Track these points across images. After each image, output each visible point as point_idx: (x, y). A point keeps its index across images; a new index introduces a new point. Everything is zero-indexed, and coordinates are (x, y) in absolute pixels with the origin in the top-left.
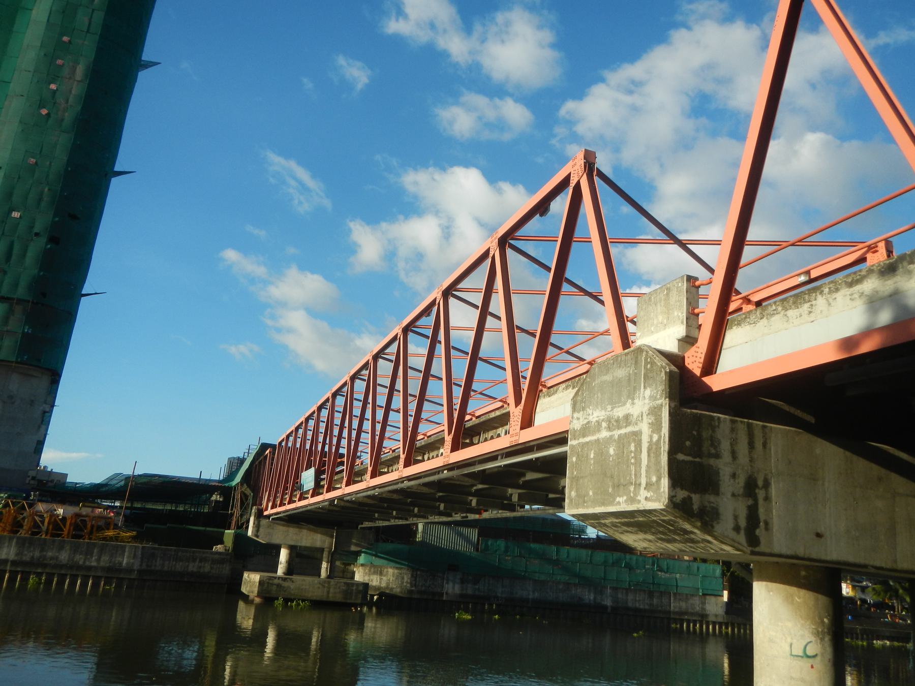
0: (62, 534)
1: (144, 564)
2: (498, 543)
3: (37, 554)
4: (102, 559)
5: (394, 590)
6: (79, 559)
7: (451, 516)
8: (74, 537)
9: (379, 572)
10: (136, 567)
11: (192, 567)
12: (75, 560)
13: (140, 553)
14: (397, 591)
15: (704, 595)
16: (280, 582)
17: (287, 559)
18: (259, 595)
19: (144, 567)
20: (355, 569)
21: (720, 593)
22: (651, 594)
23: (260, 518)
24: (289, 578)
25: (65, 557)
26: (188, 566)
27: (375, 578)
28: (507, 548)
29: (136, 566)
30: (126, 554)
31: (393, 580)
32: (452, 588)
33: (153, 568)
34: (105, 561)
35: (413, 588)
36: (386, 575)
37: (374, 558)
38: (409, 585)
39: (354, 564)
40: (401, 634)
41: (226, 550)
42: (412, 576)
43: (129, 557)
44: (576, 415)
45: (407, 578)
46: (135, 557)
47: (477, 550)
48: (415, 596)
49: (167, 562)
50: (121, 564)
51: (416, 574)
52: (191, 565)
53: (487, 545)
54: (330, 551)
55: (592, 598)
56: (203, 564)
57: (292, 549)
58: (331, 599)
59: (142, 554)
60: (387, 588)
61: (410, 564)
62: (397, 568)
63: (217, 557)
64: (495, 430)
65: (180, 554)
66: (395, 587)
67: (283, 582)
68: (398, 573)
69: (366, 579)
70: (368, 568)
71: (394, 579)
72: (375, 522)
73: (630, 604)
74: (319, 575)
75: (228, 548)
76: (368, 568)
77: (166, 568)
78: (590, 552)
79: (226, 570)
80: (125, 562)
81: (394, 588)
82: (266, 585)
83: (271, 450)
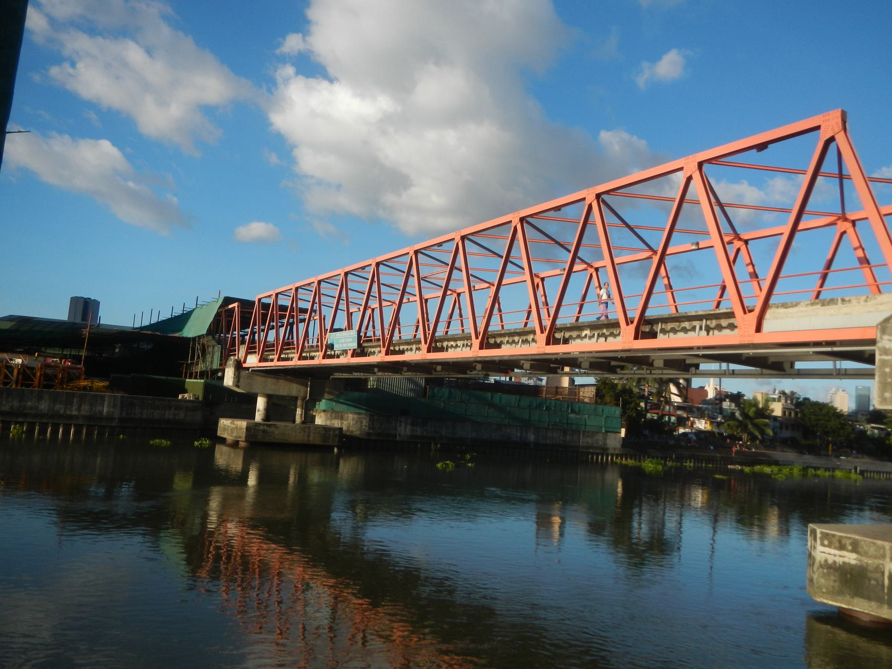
0: (33, 384)
2: (443, 390)
5: (354, 433)
7: (467, 374)
8: (45, 386)
9: (340, 417)
12: (56, 409)
14: (357, 433)
15: (607, 432)
16: (265, 427)
17: (265, 407)
18: (247, 440)
20: (314, 414)
23: (240, 369)
24: (273, 424)
25: (45, 407)
27: (337, 423)
31: (352, 424)
32: (404, 430)
35: (371, 431)
36: (347, 419)
37: (334, 403)
38: (367, 428)
39: (313, 410)
40: (361, 469)
41: (195, 398)
42: (370, 420)
44: (886, 337)
45: (365, 423)
48: (373, 438)
51: (374, 419)
54: (304, 398)
57: (269, 398)
58: (311, 443)
60: (348, 430)
61: (368, 408)
62: (356, 413)
64: (677, 324)
66: (355, 430)
67: (268, 428)
68: (357, 417)
70: (330, 414)
71: (354, 423)
72: (352, 374)
75: (197, 397)
76: (330, 414)
78: (518, 398)
81: (353, 431)
82: (252, 431)
83: (239, 305)
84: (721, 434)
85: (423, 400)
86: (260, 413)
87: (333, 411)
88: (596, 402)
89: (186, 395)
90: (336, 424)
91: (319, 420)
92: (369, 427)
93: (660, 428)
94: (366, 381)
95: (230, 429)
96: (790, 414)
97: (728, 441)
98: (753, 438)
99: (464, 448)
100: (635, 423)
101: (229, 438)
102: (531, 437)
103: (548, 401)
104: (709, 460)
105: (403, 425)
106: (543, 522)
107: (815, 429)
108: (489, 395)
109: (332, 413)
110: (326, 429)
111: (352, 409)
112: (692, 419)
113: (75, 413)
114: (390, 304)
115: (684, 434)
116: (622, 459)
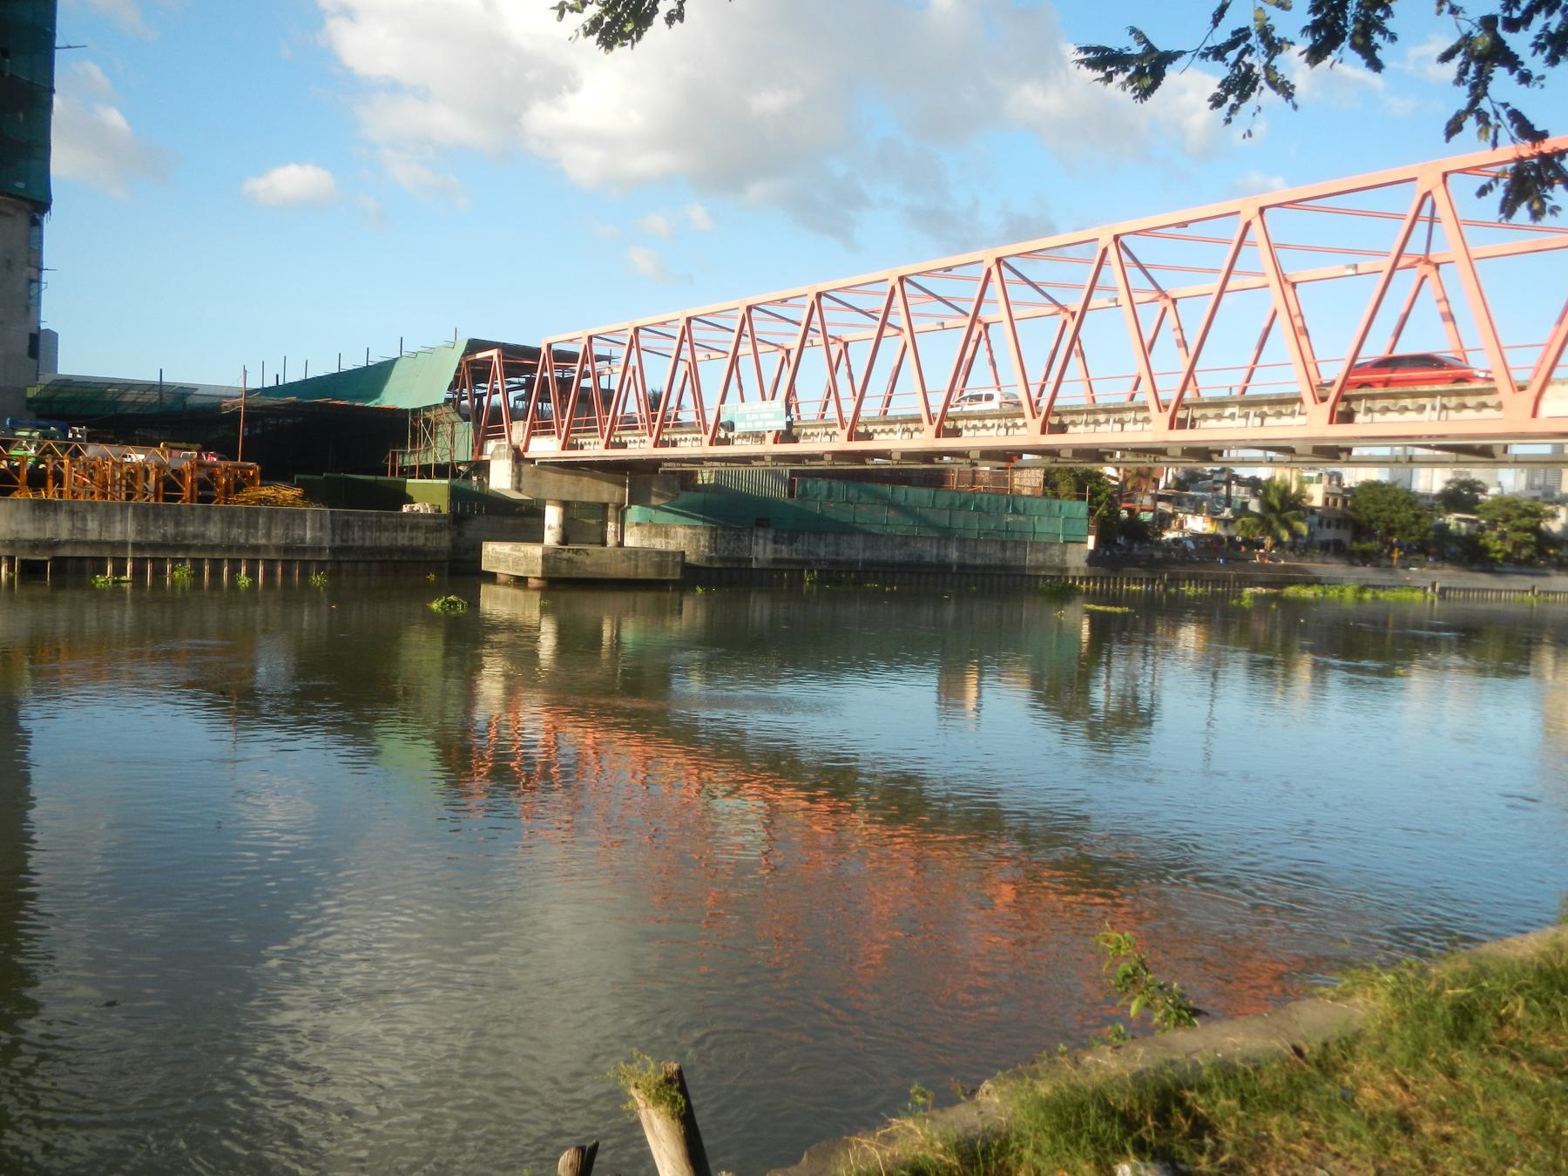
1: (337, 538)
3: (170, 530)
4: (274, 533)
6: (239, 535)
10: (326, 543)
11: (403, 539)
13: (328, 521)
19: (338, 542)
21: (1083, 539)
22: (1003, 545)
26: (396, 539)
28: (830, 490)
29: (326, 543)
30: (308, 524)
33: (350, 543)
34: (278, 535)
43: (313, 529)
46: (322, 527)
47: (791, 494)
49: (368, 534)
50: (303, 540)
52: (400, 535)
53: (805, 489)
55: (935, 551)
56: (414, 534)
59: (332, 522)
63: (431, 521)
65: (384, 520)
69: (646, 544)
73: (968, 561)
74: (604, 543)
77: (368, 543)
79: (444, 540)
80: (308, 535)
84: (1231, 539)
85: (789, 501)
86: (553, 531)
87: (652, 524)
88: (1045, 494)
89: (416, 507)
90: (659, 544)
91: (630, 541)
92: (709, 547)
93: (1137, 531)
94: (693, 474)
95: (510, 560)
96: (1335, 503)
97: (1243, 549)
98: (1278, 543)
99: (853, 575)
100: (1109, 530)
101: (502, 570)
102: (953, 554)
103: (978, 496)
104: (1217, 582)
105: (761, 542)
106: (950, 692)
107: (1374, 526)
108: (888, 488)
109: (651, 527)
110: (635, 551)
111: (683, 520)
112: (1181, 515)
113: (262, 541)
114: (774, 348)
115: (1176, 541)
116: (1088, 584)
